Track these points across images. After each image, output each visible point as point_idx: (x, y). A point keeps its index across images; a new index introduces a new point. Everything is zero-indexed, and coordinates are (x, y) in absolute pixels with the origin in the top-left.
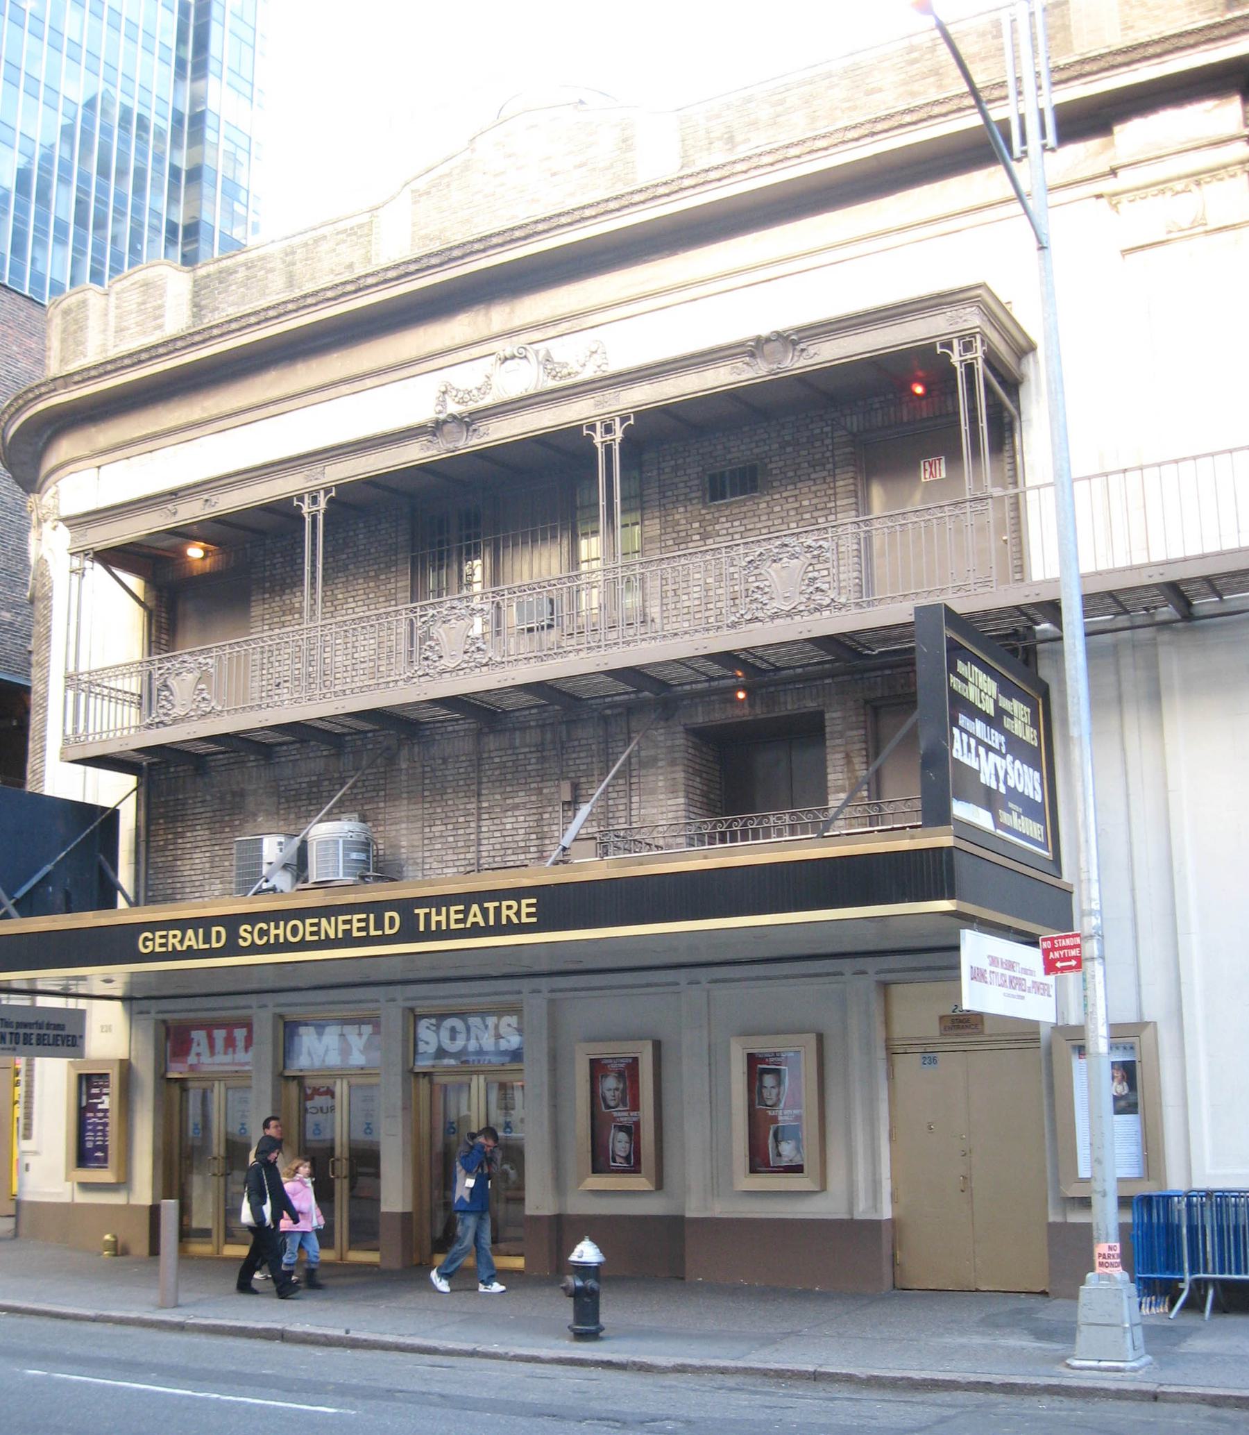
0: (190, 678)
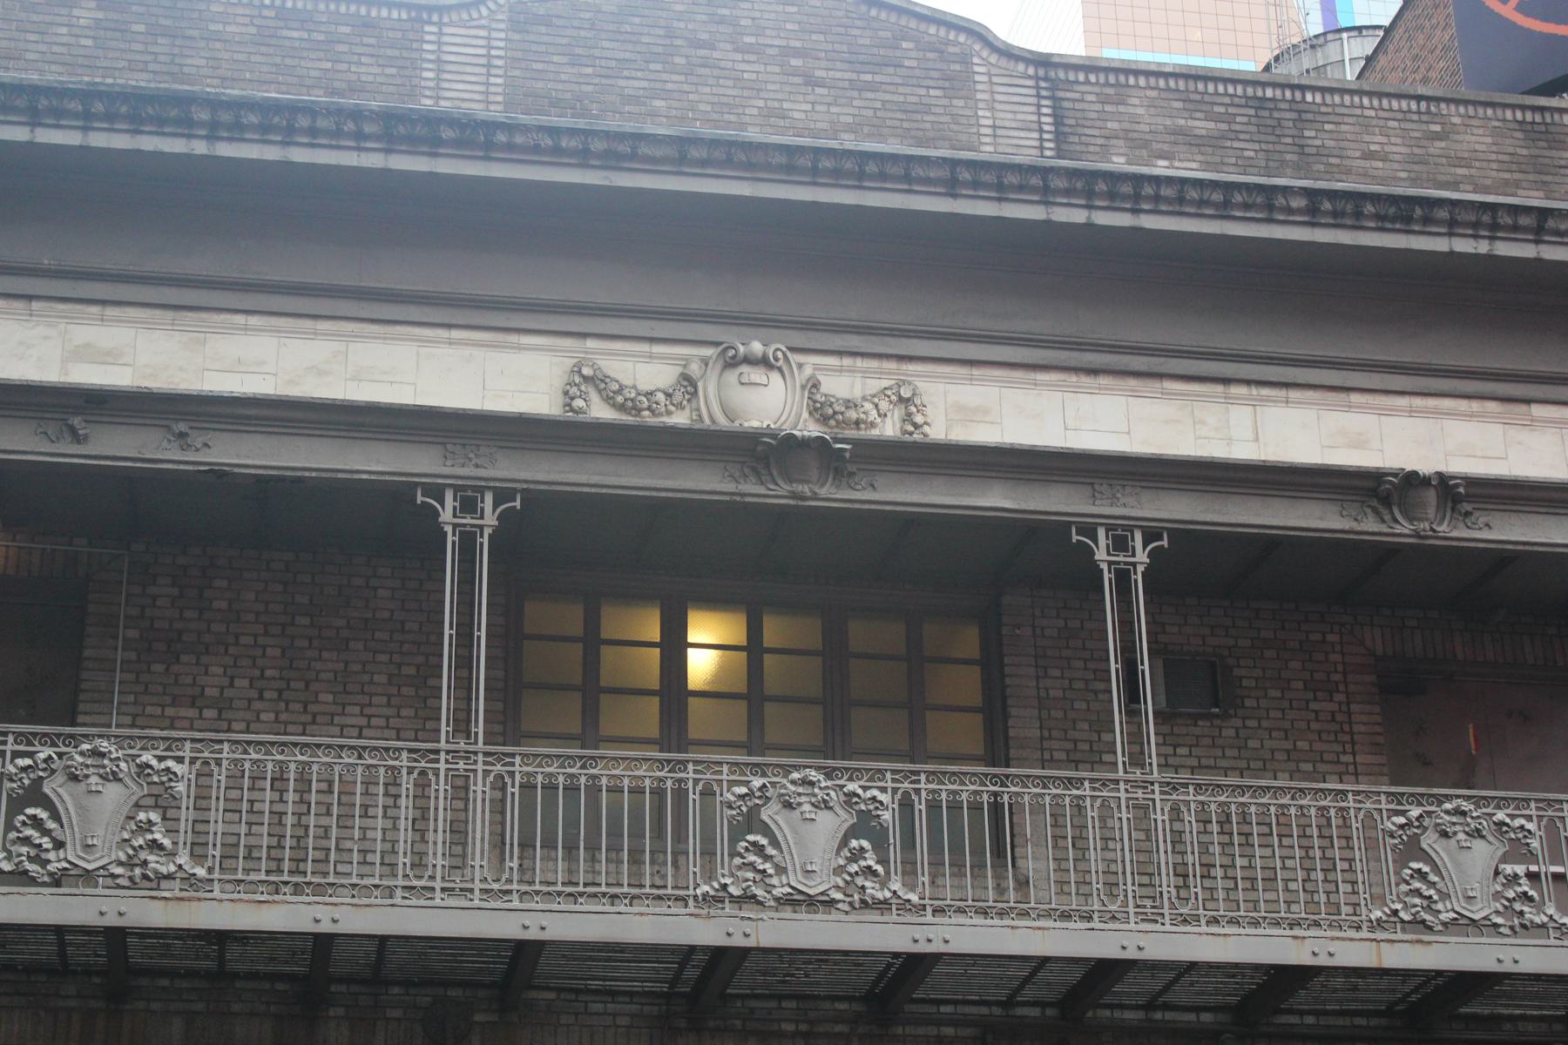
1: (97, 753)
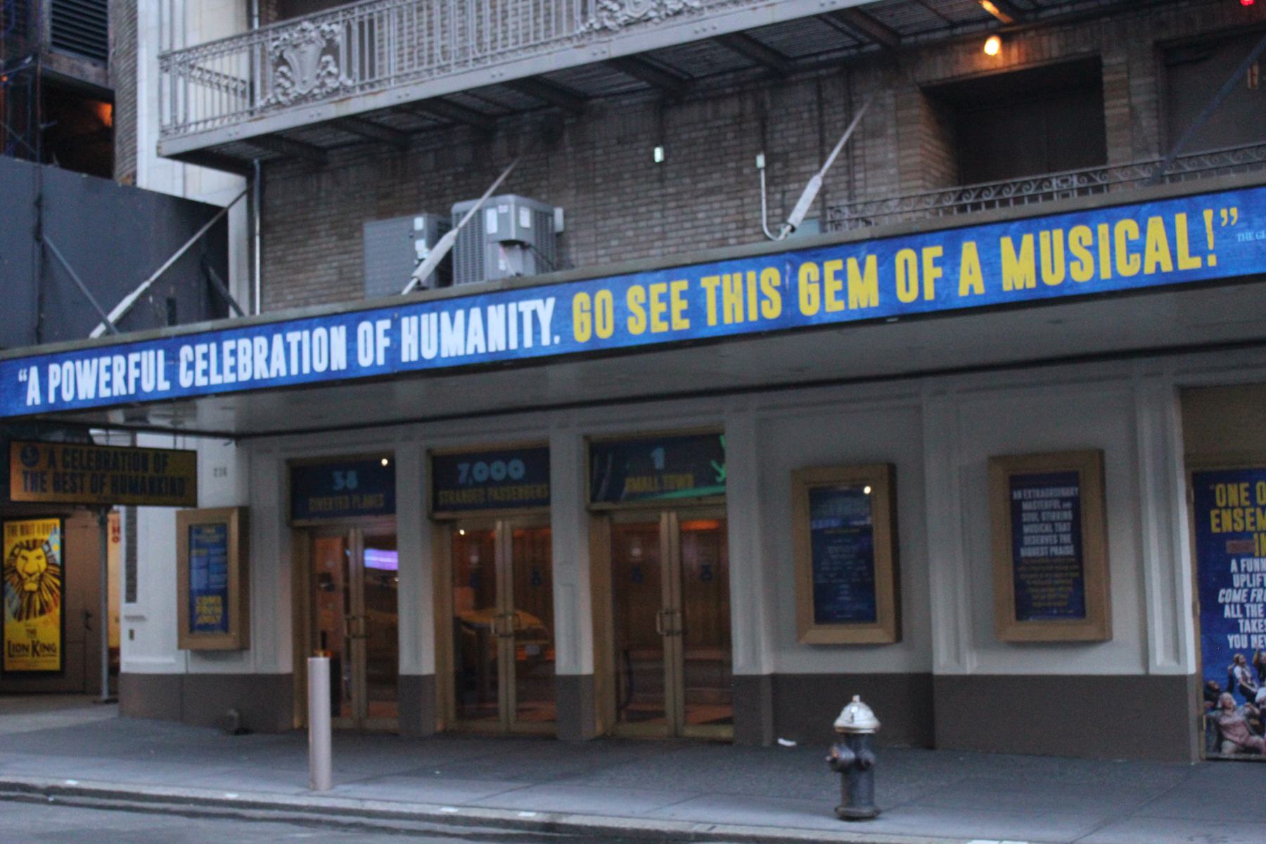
0: (311, 51)
1: (303, 30)
